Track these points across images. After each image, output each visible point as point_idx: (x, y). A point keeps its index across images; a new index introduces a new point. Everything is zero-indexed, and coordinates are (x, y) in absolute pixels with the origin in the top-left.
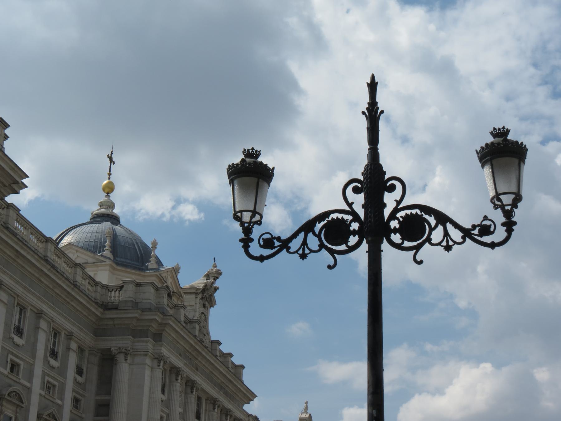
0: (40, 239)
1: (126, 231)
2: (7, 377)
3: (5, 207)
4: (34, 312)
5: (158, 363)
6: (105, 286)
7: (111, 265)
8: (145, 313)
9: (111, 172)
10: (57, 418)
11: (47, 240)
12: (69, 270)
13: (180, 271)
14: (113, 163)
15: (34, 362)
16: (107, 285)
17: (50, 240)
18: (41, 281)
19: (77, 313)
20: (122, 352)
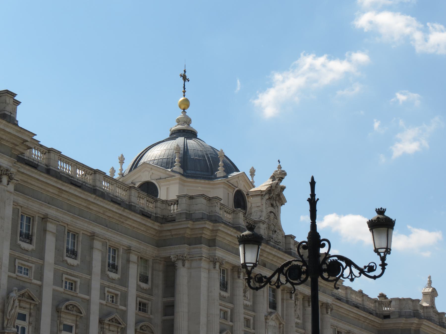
0: (88, 172)
1: (198, 144)
2: (64, 293)
3: (46, 152)
4: (88, 235)
5: (214, 265)
6: (165, 202)
7: (180, 178)
9: (186, 90)
10: (120, 321)
11: (95, 172)
12: (124, 193)
14: (187, 81)
15: (91, 277)
16: (167, 201)
17: (98, 172)
18: (89, 208)
19: (134, 230)
20: (180, 259)
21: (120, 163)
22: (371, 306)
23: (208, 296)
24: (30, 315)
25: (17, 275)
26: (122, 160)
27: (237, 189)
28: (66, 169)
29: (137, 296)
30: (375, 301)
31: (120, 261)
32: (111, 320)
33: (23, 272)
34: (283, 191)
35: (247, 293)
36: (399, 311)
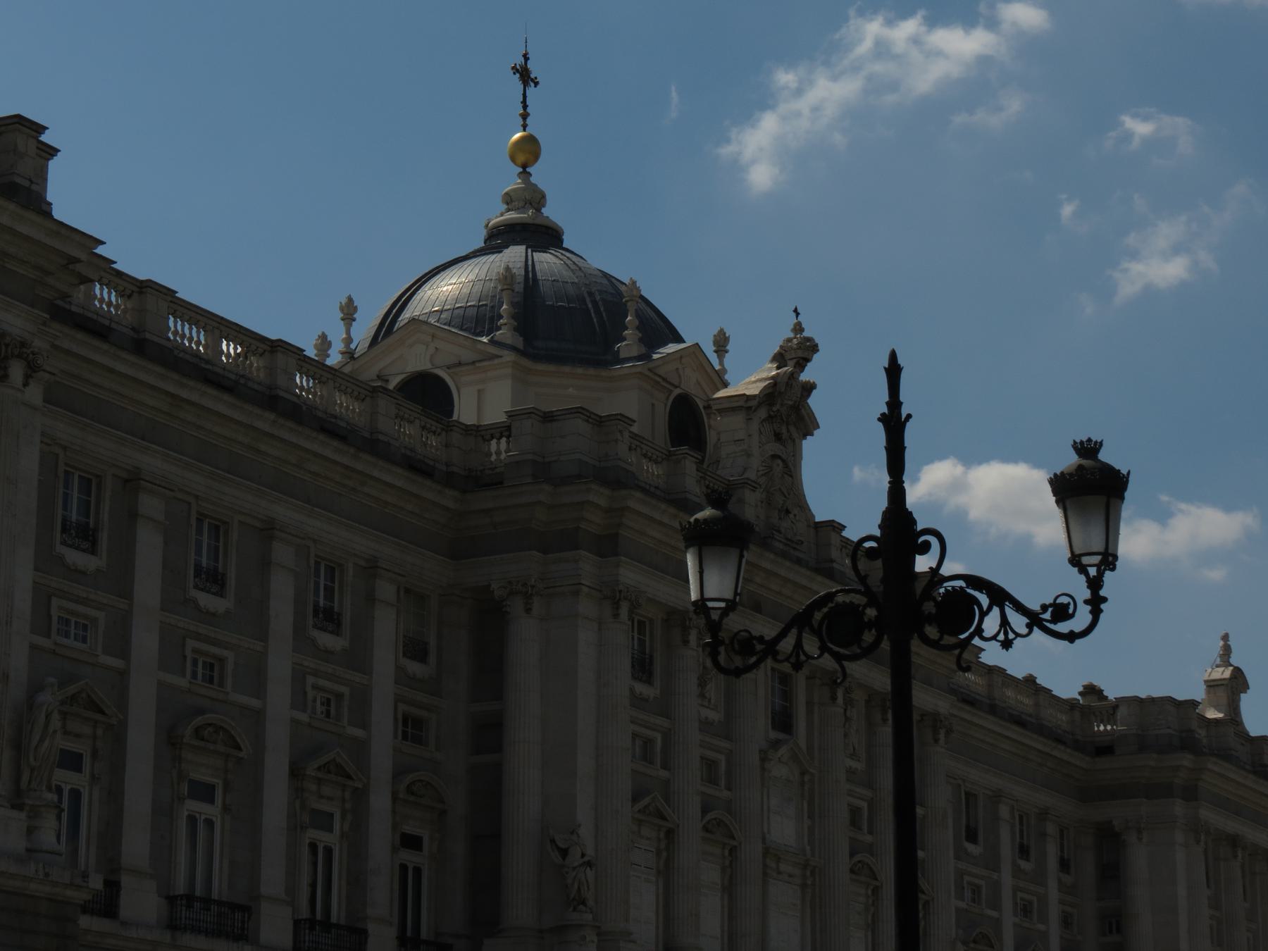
0: (253, 347)
1: (567, 265)
6: (472, 430)
9: (529, 110)
11: (272, 347)
12: (357, 407)
13: (728, 348)
14: (532, 84)
16: (478, 426)
17: (282, 347)
21: (343, 319)
22: (1062, 719)
25: (56, 644)
26: (349, 312)
27: (677, 391)
28: (193, 338)
30: (1071, 705)
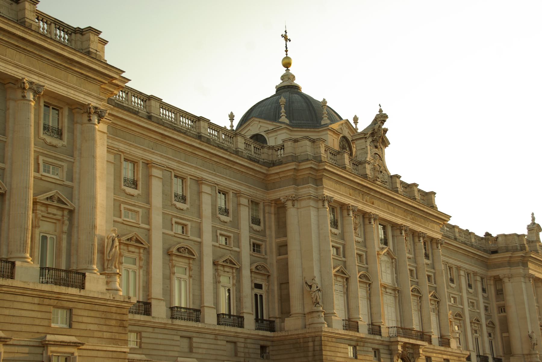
2: (175, 236)
8: (302, 164)
9: (288, 49)
13: (358, 121)
14: (289, 41)
20: (290, 200)
21: (230, 120)
23: (319, 233)
24: (140, 259)
26: (232, 117)
27: (341, 135)
29: (251, 238)
31: (231, 205)
32: (225, 261)
33: (130, 217)
34: (386, 133)
35: (358, 230)
36: (506, 245)
